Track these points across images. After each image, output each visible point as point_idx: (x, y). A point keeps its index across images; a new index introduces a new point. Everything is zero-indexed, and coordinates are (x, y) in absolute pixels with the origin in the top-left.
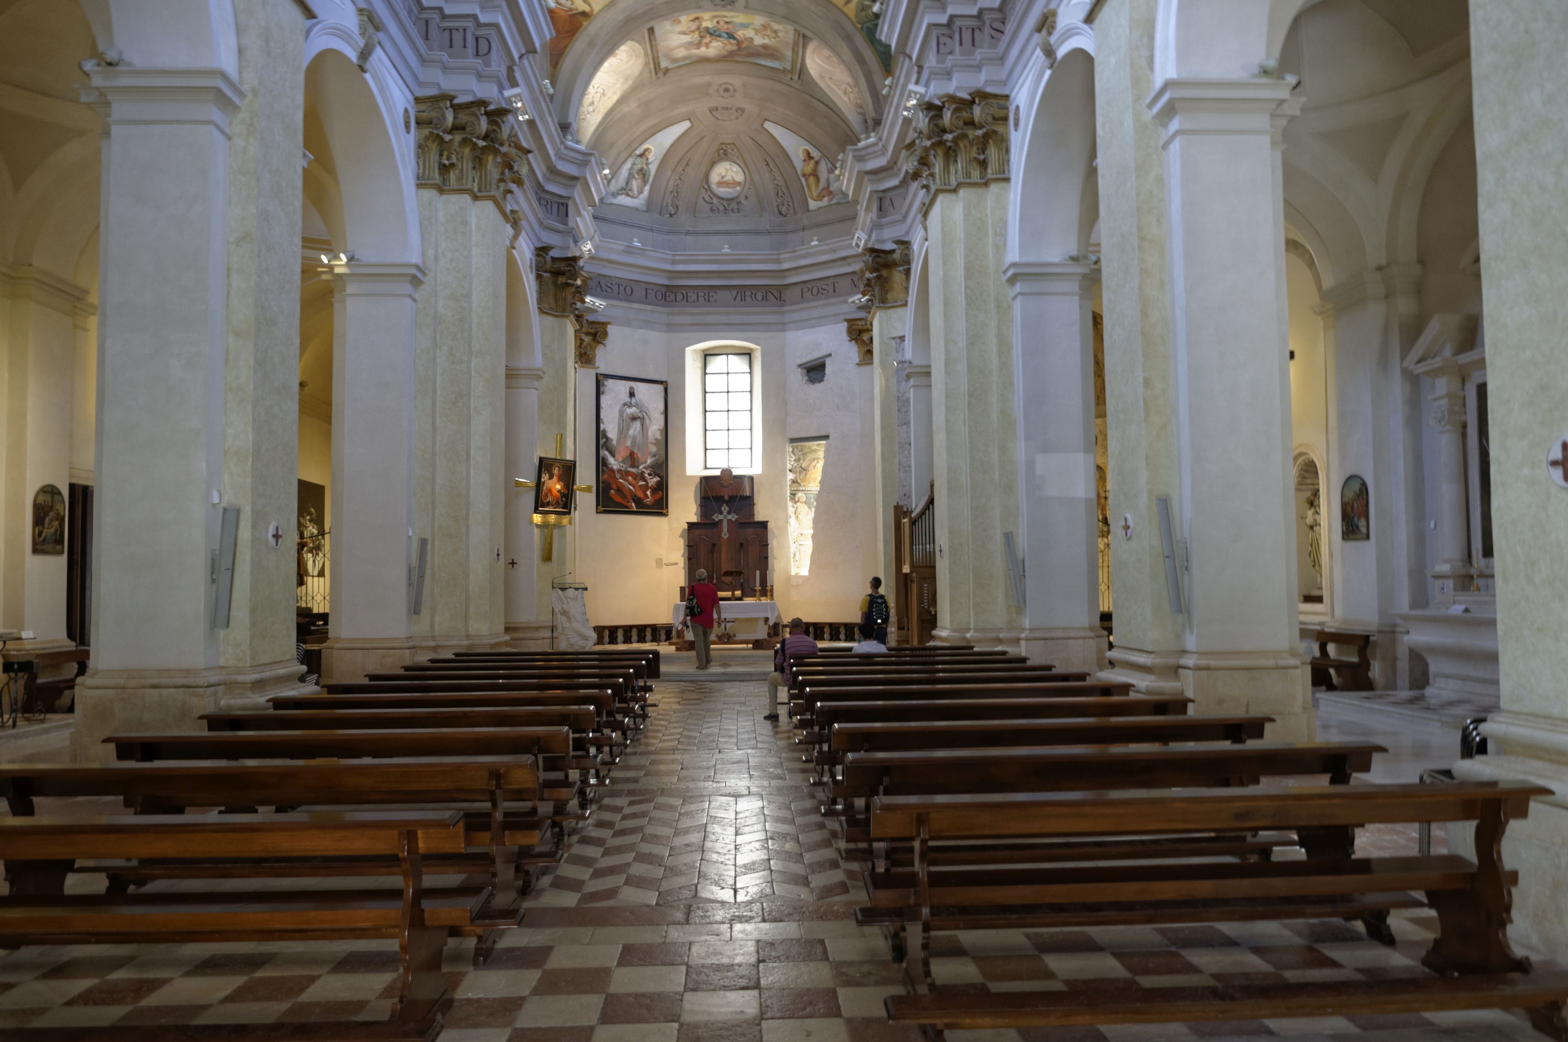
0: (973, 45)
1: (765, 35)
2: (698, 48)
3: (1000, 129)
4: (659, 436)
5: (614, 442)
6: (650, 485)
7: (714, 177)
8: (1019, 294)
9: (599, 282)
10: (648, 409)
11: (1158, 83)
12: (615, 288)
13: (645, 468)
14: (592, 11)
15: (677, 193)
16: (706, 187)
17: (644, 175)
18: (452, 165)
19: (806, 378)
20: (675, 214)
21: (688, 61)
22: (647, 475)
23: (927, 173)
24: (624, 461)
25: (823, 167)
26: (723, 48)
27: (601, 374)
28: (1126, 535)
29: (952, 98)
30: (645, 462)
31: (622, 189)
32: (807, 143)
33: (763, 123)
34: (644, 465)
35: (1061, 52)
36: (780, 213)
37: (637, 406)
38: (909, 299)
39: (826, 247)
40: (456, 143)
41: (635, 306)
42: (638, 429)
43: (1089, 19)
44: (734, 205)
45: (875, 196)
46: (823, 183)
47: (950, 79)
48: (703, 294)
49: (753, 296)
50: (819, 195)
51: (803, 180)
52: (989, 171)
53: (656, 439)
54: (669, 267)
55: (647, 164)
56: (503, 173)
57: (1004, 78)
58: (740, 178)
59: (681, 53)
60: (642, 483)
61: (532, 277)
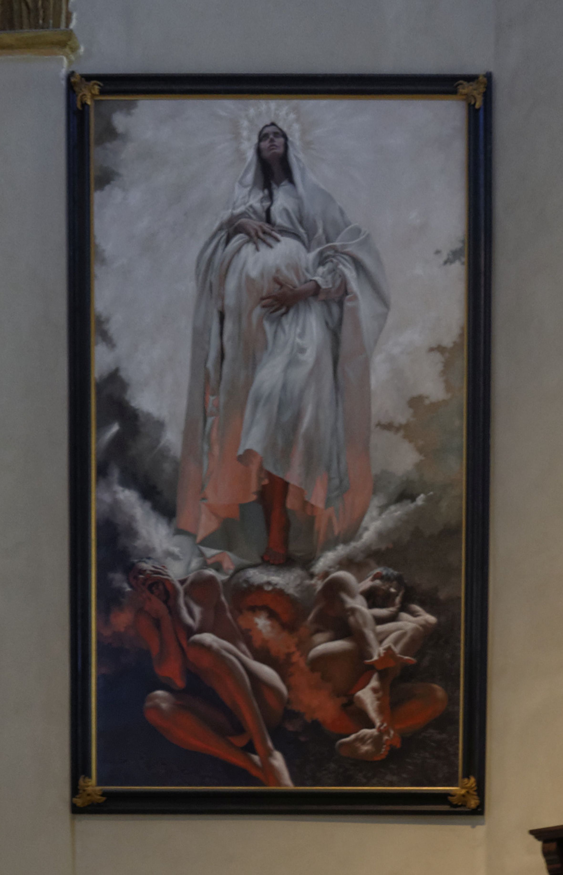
27: (88, 78)
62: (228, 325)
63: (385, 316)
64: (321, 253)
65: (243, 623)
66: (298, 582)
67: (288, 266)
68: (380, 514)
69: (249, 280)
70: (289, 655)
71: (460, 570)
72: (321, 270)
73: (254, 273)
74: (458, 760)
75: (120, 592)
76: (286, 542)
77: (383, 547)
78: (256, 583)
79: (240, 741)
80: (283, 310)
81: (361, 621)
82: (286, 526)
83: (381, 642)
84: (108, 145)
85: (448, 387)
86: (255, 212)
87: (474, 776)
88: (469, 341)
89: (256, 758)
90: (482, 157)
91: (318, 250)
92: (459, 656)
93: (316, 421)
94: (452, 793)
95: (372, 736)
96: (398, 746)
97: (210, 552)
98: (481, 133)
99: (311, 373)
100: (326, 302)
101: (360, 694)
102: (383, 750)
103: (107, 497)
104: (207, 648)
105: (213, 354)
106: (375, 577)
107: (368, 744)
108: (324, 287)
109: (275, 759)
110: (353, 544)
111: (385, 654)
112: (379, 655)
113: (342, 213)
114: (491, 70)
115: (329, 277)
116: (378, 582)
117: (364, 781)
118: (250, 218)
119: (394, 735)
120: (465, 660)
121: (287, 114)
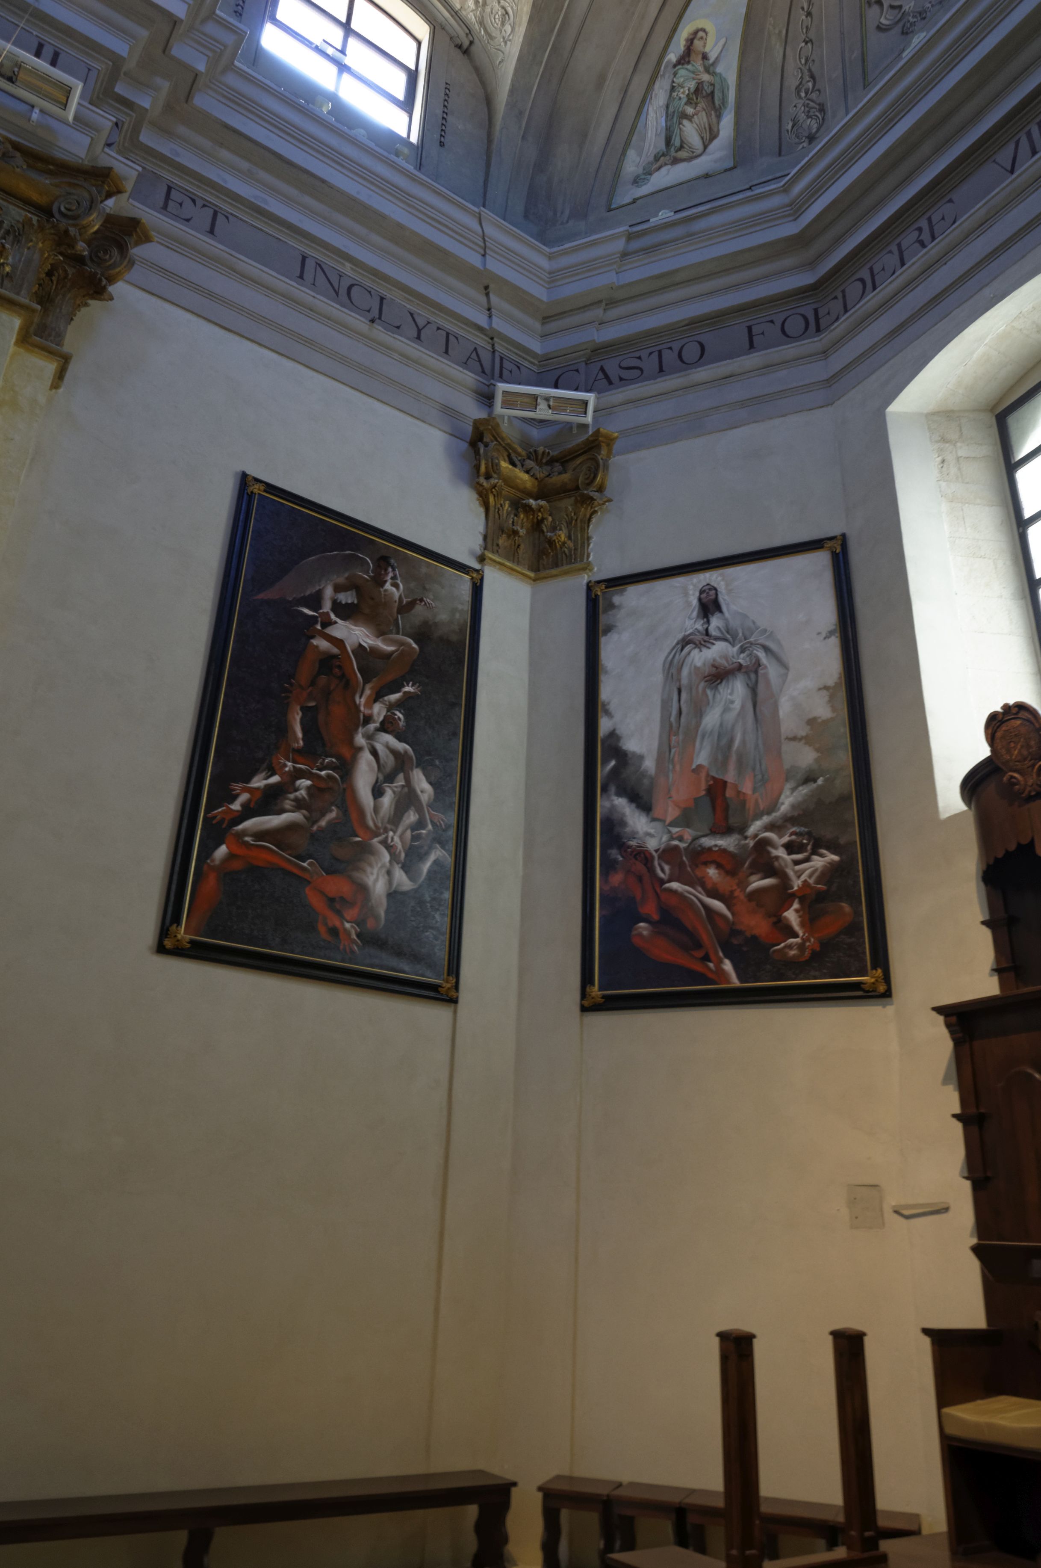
4: (822, 710)
5: (649, 764)
6: (797, 884)
9: (602, 369)
10: (771, 636)
13: (771, 827)
22: (781, 853)
24: (685, 819)
27: (599, 582)
30: (773, 807)
34: (766, 819)
37: (729, 635)
42: (737, 705)
53: (812, 722)
54: (790, 229)
60: (758, 883)
62: (684, 695)
63: (786, 675)
64: (741, 647)
65: (699, 873)
66: (737, 842)
67: (721, 657)
68: (792, 793)
69: (697, 669)
70: (732, 892)
71: (854, 823)
72: (742, 656)
73: (699, 664)
74: (866, 956)
75: (615, 861)
76: (726, 818)
77: (796, 814)
78: (707, 847)
79: (699, 954)
80: (719, 681)
81: (783, 864)
82: (726, 808)
83: (799, 877)
84: (610, 613)
85: (834, 709)
86: (699, 631)
87: (881, 968)
88: (845, 681)
89: (711, 965)
90: (843, 577)
91: (740, 645)
92: (860, 881)
93: (743, 742)
94: (864, 982)
95: (797, 944)
96: (818, 949)
97: (675, 830)
98: (842, 565)
99: (739, 714)
100: (747, 673)
101: (786, 914)
102: (807, 953)
103: (607, 804)
104: (674, 892)
105: (674, 712)
106: (791, 834)
107: (795, 950)
108: (744, 664)
109: (725, 964)
110: (774, 815)
111: (803, 885)
112: (798, 886)
113: (754, 623)
114: (844, 531)
115: (748, 659)
116: (794, 837)
117: (794, 976)
118: (696, 635)
119: (814, 942)
120: (865, 884)
121: (716, 578)
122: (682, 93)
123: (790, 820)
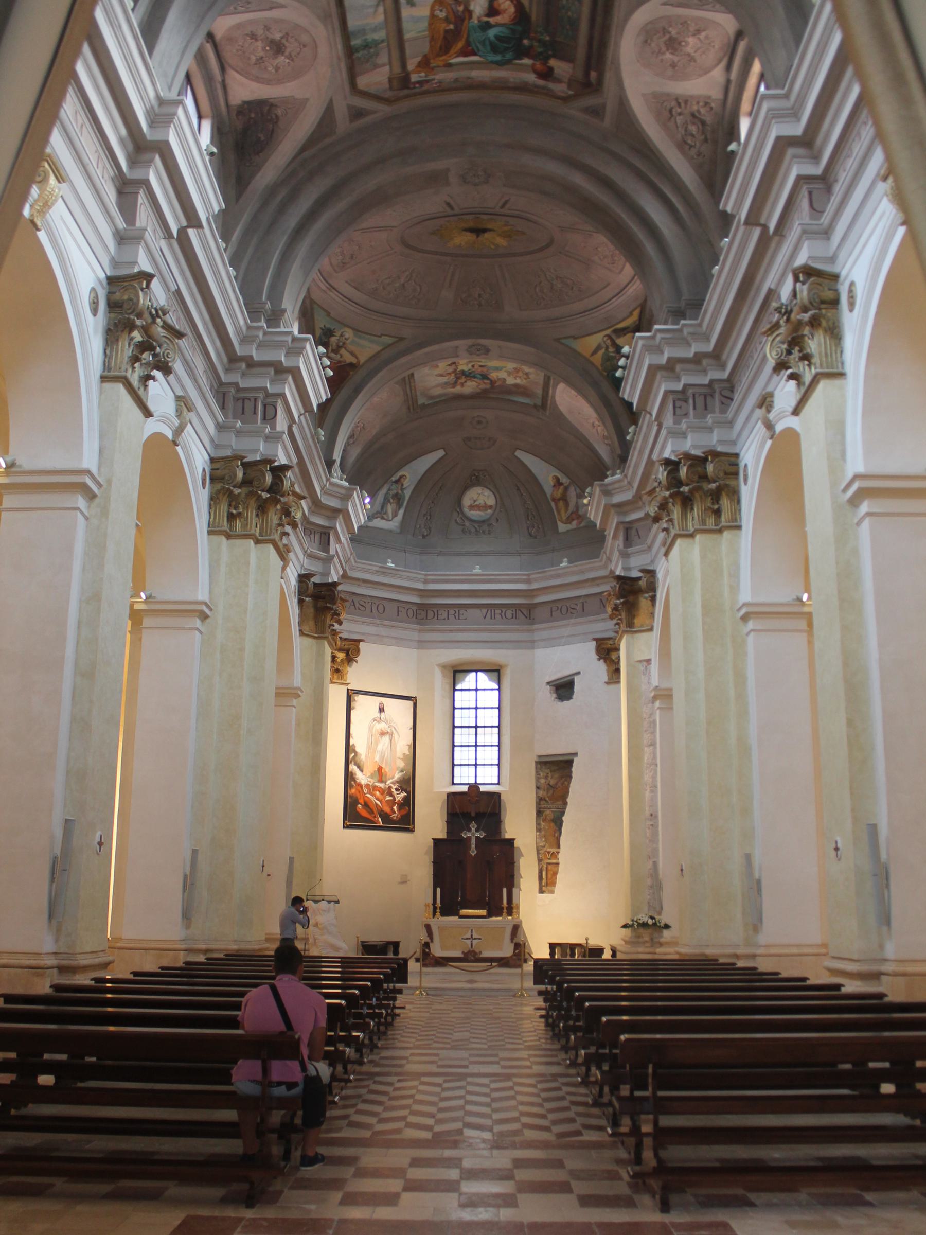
0: (706, 408)
1: (517, 376)
2: (454, 387)
3: (732, 483)
4: (407, 752)
5: (363, 757)
6: (397, 800)
7: (467, 501)
8: (752, 630)
11: (849, 475)
12: (368, 606)
13: (392, 783)
14: (359, 362)
15: (430, 516)
16: (458, 510)
17: (399, 499)
18: (239, 515)
19: (555, 695)
20: (427, 535)
21: (443, 398)
22: (394, 790)
23: (667, 519)
24: (372, 776)
25: (572, 493)
26: (478, 386)
27: (351, 690)
28: (837, 857)
29: (687, 456)
31: (377, 513)
32: (558, 471)
33: (514, 452)
34: (391, 780)
35: (779, 428)
36: (530, 534)
38: (655, 625)
39: (576, 569)
40: (243, 495)
41: (386, 623)
42: (386, 744)
43: (796, 412)
44: (485, 527)
45: (621, 527)
46: (571, 508)
47: (686, 438)
48: (454, 612)
49: (503, 614)
50: (568, 518)
51: (553, 504)
52: (723, 519)
53: (404, 754)
54: (421, 586)
55: (402, 489)
56: (281, 518)
57: (734, 437)
58: (491, 501)
59: (438, 391)
60: (388, 798)
61: (295, 601)
79: (373, 815)
122: (391, 493)
123: (397, 782)
